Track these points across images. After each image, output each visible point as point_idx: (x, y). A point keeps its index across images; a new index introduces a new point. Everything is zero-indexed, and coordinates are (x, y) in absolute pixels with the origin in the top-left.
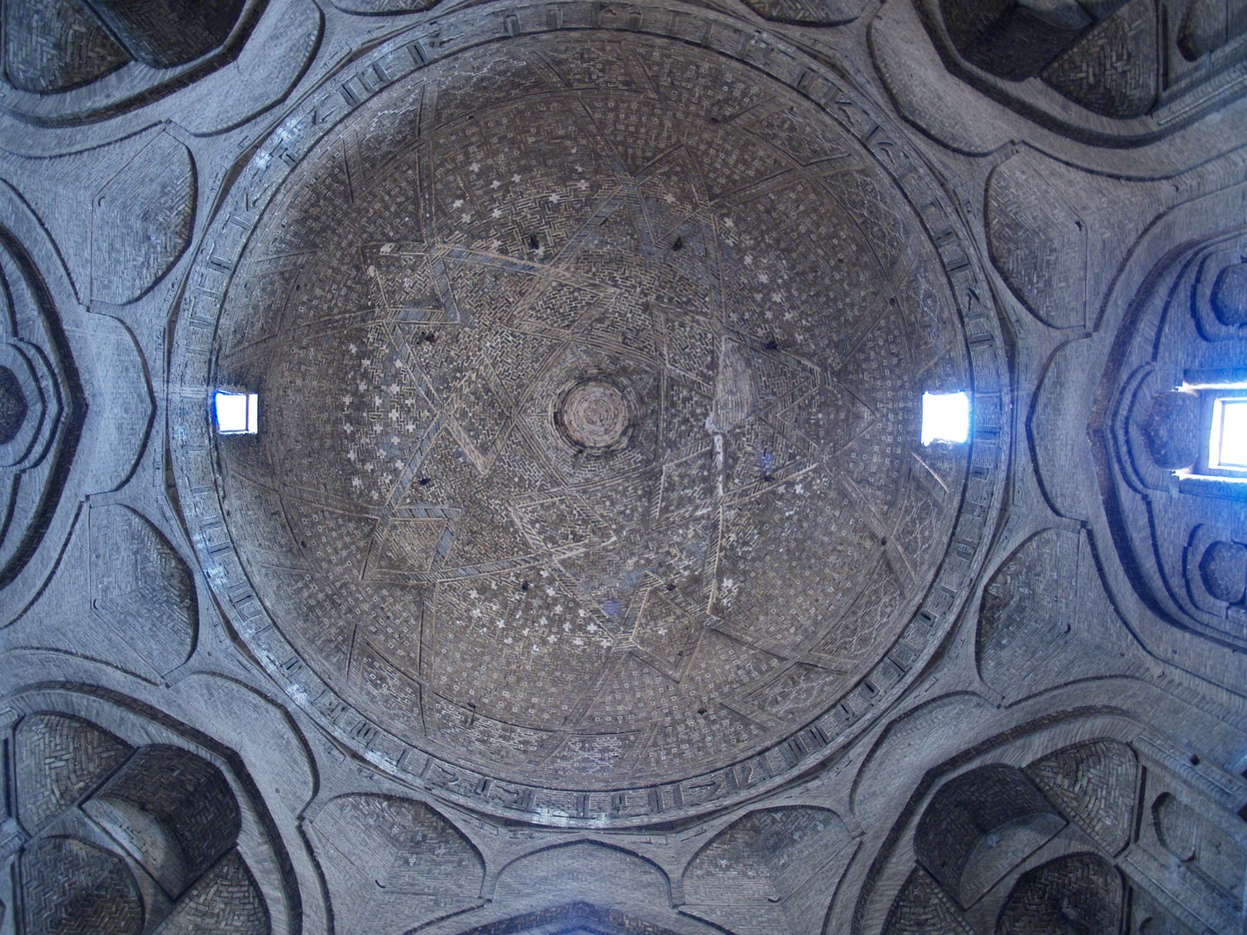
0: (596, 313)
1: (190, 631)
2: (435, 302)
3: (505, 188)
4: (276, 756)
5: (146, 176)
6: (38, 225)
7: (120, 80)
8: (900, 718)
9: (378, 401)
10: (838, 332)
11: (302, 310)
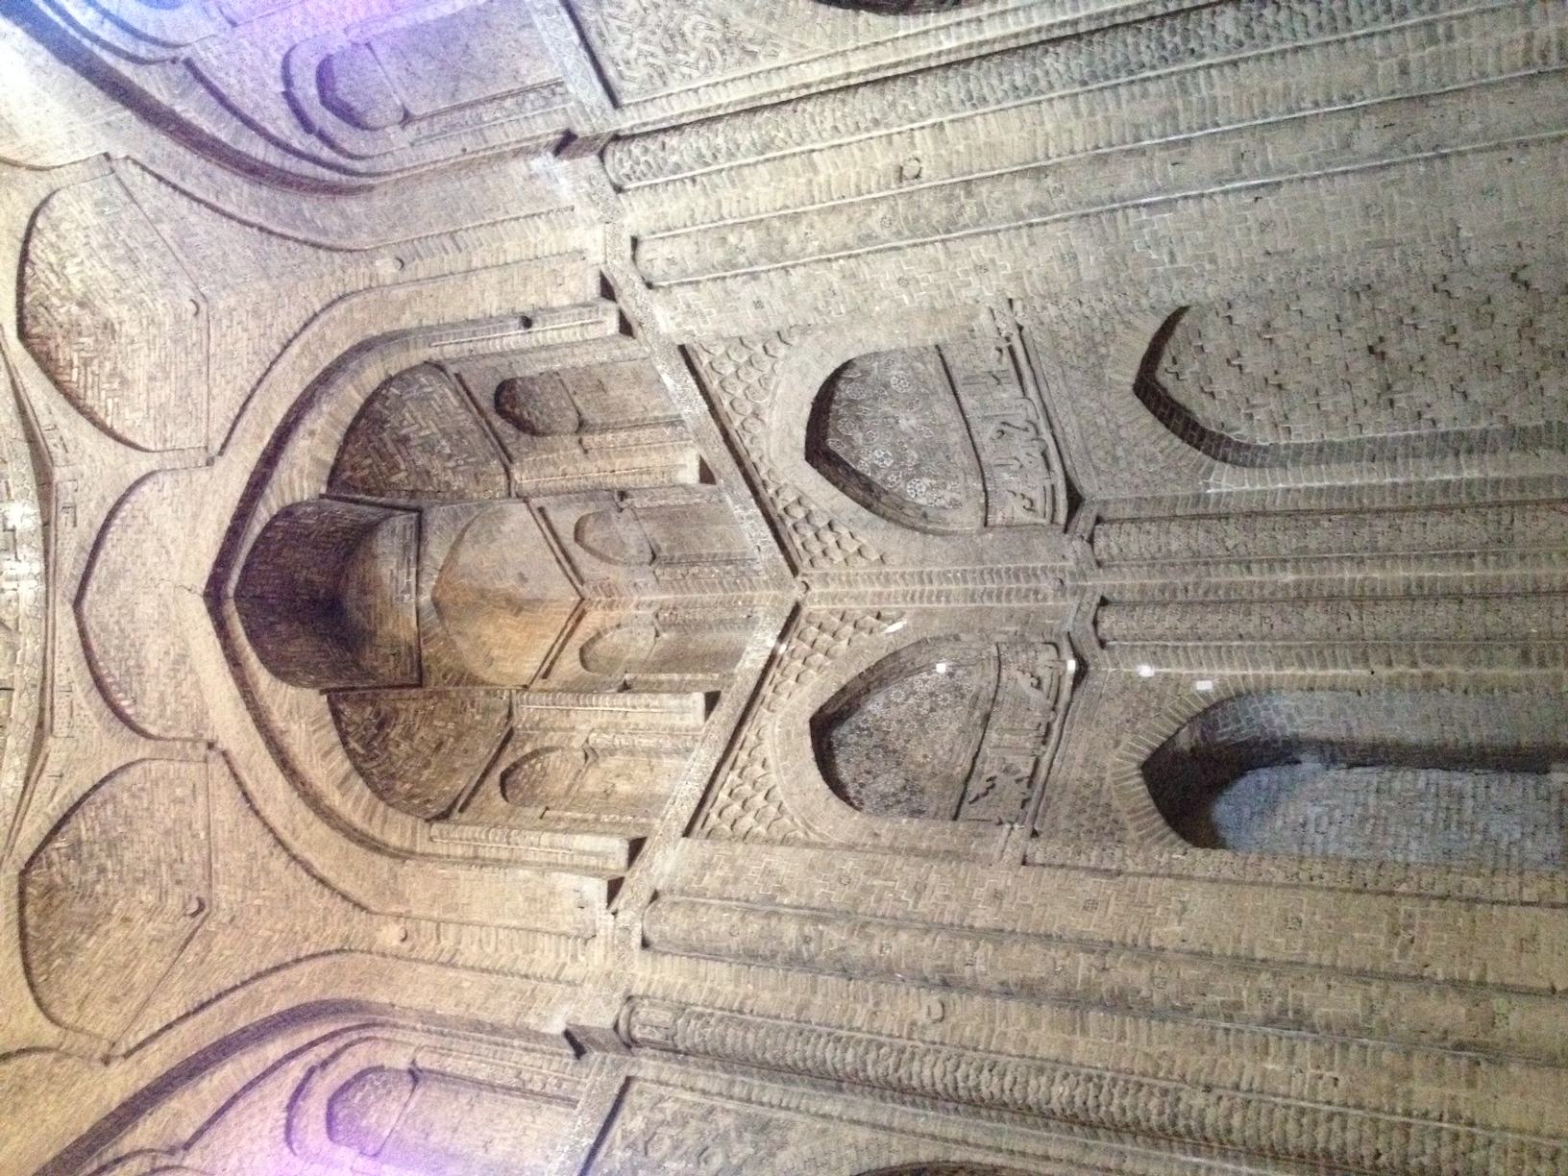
5: (167, 378)
6: (265, 224)
7: (317, 461)
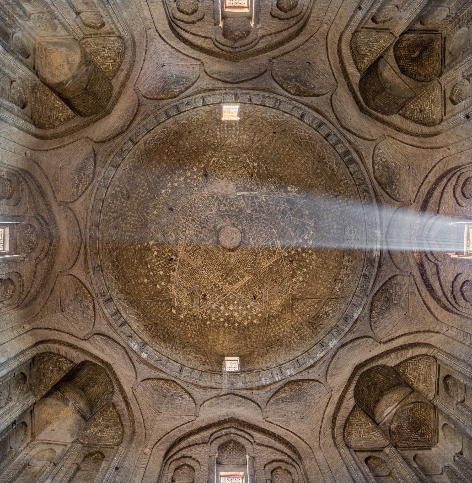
1: (311, 382)
2: (192, 294)
3: (153, 270)
4: (357, 351)
8: (340, 123)
9: (227, 314)
10: (200, 152)
11: (195, 341)
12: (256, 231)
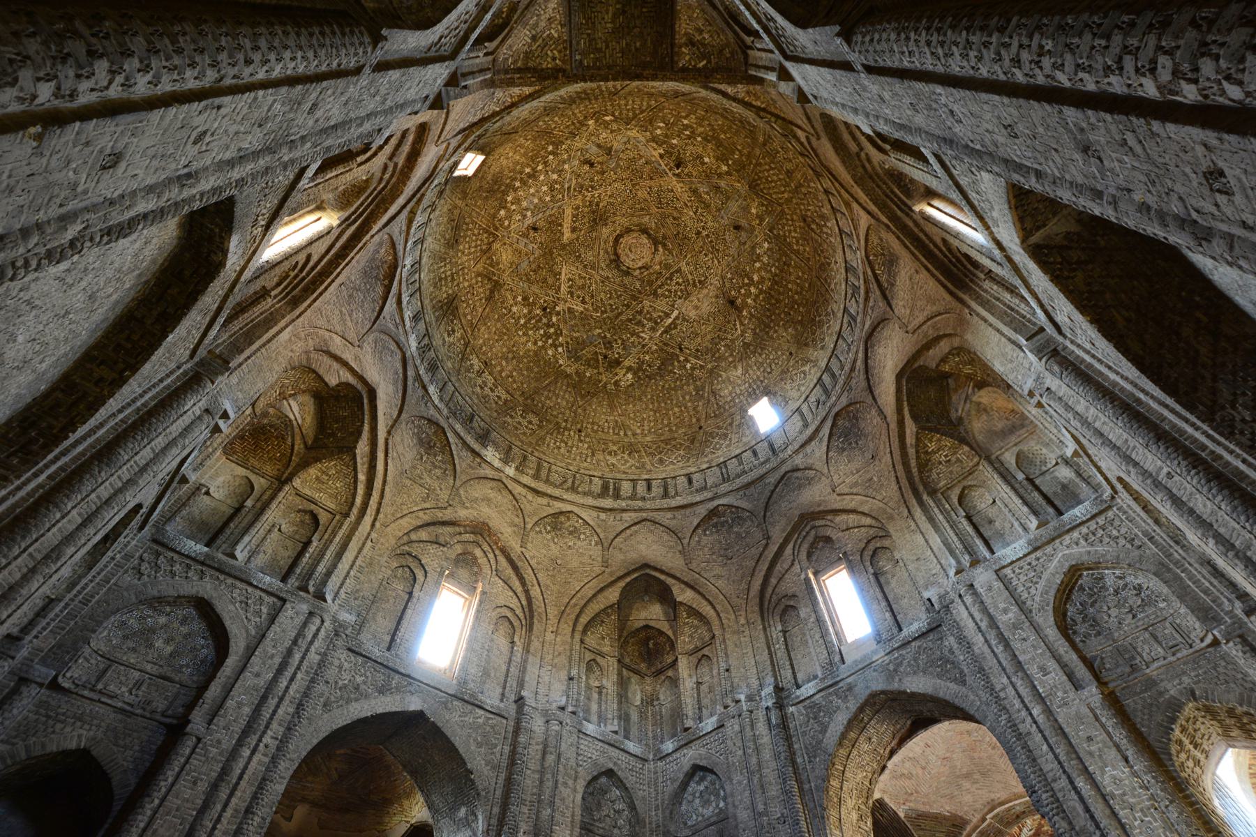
0: (675, 214)
9: (542, 178)
12: (616, 291)
